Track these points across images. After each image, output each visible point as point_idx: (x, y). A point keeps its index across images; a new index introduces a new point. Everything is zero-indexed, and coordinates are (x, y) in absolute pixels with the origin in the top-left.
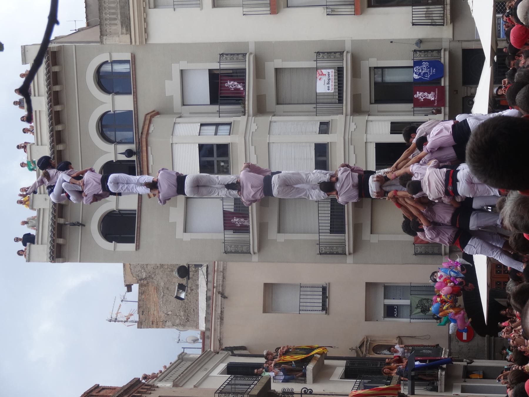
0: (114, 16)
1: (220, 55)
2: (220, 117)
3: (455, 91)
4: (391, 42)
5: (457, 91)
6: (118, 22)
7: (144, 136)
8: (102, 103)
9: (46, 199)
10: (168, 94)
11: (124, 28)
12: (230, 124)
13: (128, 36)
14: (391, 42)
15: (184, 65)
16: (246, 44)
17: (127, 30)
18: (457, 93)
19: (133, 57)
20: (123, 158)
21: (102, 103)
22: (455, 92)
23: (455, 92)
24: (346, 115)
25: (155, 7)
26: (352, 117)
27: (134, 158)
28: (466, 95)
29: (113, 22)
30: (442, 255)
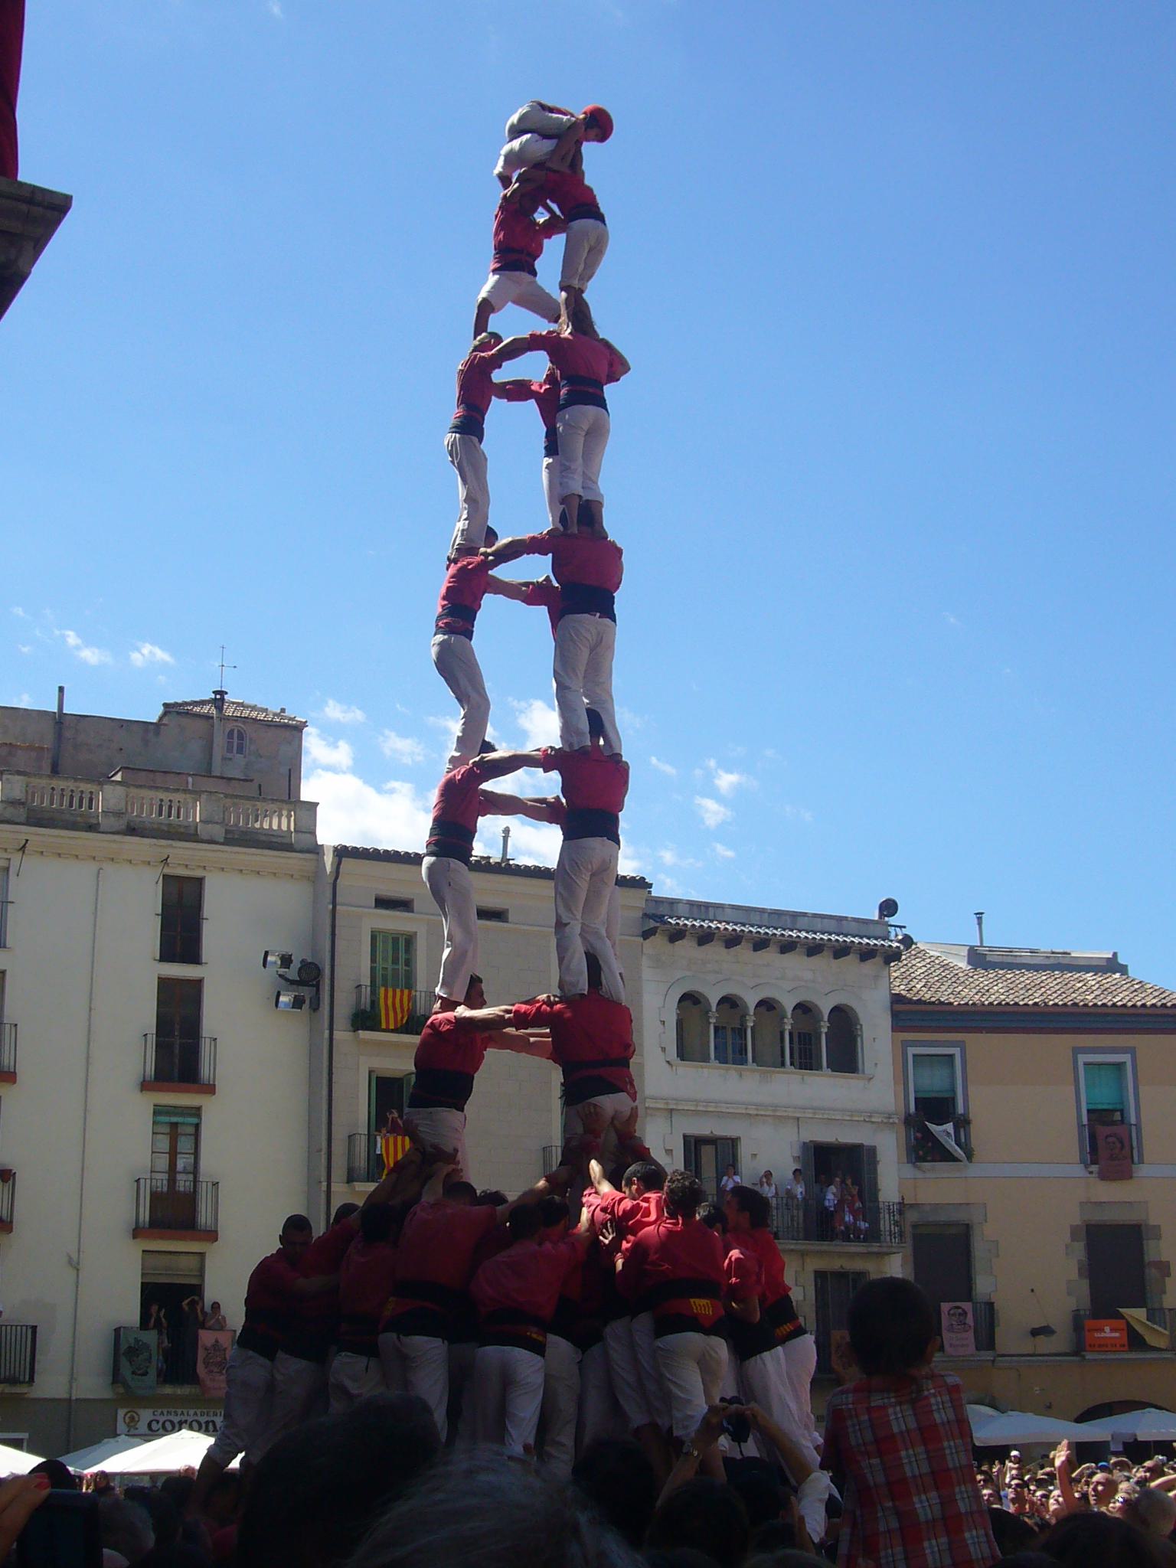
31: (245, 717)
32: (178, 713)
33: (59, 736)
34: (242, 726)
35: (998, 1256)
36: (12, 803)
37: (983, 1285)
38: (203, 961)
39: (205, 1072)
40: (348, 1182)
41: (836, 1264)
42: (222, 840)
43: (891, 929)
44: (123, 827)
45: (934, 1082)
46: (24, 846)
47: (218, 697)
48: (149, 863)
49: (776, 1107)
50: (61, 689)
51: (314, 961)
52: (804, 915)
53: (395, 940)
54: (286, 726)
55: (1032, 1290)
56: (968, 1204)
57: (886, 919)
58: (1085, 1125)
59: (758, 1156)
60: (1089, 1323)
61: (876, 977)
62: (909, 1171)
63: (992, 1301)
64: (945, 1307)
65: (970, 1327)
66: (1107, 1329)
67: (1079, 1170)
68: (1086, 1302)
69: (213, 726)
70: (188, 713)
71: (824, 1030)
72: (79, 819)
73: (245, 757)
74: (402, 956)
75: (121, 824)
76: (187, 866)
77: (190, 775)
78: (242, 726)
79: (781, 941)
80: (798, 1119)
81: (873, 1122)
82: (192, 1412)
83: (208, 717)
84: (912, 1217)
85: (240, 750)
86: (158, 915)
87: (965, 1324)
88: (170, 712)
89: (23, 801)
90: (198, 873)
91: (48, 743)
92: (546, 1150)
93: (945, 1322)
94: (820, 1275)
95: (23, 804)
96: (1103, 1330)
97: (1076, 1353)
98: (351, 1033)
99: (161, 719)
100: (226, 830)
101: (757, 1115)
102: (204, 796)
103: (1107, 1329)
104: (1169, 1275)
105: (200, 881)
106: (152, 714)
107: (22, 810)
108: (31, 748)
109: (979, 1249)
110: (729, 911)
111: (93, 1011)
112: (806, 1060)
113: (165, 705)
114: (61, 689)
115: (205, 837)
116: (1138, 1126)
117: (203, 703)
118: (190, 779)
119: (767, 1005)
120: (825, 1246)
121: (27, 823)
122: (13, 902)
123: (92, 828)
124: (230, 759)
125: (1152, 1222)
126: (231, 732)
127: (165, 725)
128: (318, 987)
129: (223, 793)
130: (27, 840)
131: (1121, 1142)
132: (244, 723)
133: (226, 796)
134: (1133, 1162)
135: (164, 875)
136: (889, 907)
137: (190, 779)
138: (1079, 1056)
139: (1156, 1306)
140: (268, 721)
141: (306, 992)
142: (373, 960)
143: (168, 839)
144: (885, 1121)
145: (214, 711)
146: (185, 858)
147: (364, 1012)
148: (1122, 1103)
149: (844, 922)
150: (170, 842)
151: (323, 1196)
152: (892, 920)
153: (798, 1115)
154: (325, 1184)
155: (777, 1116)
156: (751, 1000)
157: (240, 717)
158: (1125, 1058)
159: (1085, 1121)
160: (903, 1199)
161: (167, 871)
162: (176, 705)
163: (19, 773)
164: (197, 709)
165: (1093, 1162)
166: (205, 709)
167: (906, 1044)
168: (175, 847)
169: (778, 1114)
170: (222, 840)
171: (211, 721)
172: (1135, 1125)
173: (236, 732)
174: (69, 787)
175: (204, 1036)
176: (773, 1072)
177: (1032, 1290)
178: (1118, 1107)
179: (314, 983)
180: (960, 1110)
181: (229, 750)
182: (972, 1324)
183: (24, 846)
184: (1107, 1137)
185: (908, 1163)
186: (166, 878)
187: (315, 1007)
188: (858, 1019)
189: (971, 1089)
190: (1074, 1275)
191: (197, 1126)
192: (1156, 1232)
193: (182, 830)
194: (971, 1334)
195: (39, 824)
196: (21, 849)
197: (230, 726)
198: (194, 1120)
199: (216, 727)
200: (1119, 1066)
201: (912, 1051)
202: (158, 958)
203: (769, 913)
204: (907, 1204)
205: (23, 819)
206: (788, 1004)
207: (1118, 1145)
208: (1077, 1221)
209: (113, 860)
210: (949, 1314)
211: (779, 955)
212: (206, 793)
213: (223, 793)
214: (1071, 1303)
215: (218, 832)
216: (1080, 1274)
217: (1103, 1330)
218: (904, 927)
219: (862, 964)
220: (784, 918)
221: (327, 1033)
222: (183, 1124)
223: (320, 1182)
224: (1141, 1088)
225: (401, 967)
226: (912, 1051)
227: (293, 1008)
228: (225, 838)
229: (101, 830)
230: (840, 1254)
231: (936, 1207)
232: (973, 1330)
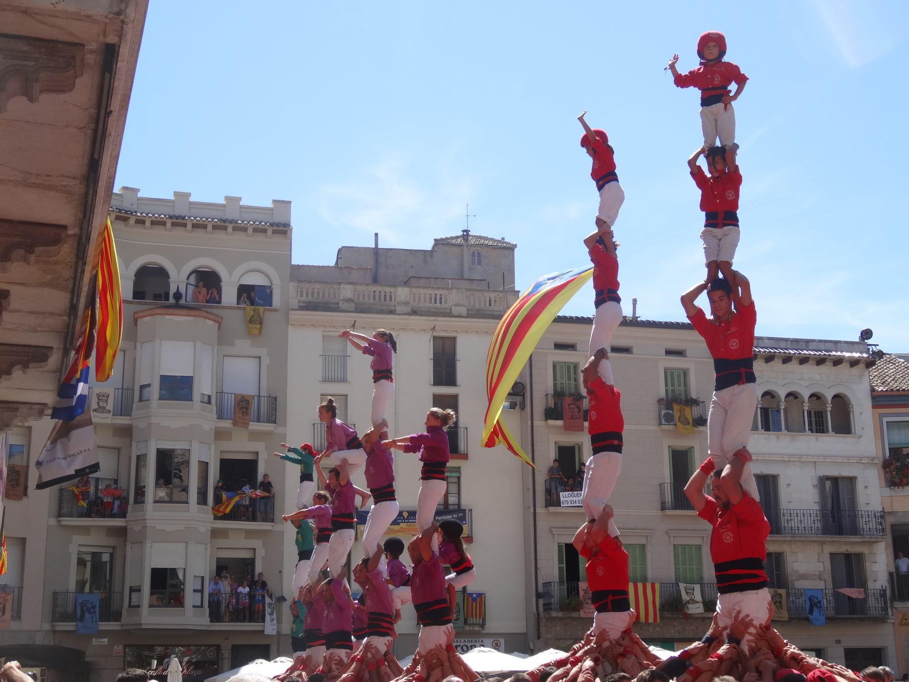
0: (315, 296)
1: (276, 398)
2: (216, 393)
3: (228, 636)
4: (280, 572)
5: (227, 639)
6: (310, 299)
7: (205, 314)
8: (230, 274)
9: (132, 204)
10: (237, 342)
11: (304, 305)
12: (209, 402)
13: (297, 308)
14: (280, 572)
15: (266, 361)
16: (284, 424)
17: (302, 307)
18: (226, 639)
19: (276, 310)
20: (173, 290)
21: (230, 274)
22: (226, 637)
23: (226, 637)
24: (213, 523)
25: (323, 336)
26: (211, 529)
27: (172, 300)
28: (222, 648)
29: (299, 294)
30: (52, 622)
31: (481, 244)
32: (443, 244)
33: (377, 261)
34: (480, 249)
36: (347, 300)
38: (458, 384)
39: (462, 447)
40: (546, 507)
41: (843, 549)
42: (465, 315)
43: (870, 347)
44: (410, 311)
46: (354, 325)
47: (465, 233)
48: (425, 330)
49: (801, 456)
50: (376, 235)
51: (522, 382)
52: (813, 341)
53: (569, 367)
54: (505, 248)
57: (866, 341)
59: (791, 486)
61: (861, 376)
62: (887, 491)
69: (463, 250)
70: (448, 244)
71: (829, 409)
72: (384, 307)
73: (482, 267)
74: (572, 376)
75: (408, 309)
76: (446, 331)
77: (450, 279)
78: (480, 249)
79: (799, 357)
80: (815, 462)
81: (862, 463)
82: (462, 640)
83: (460, 245)
84: (890, 520)
85: (479, 263)
86: (431, 359)
88: (438, 244)
89: (352, 299)
90: (453, 335)
91: (370, 264)
92: (661, 485)
94: (833, 555)
95: (353, 301)
98: (543, 422)
99: (433, 248)
100: (468, 309)
101: (789, 461)
102: (454, 291)
105: (454, 339)
106: (428, 246)
107: (352, 304)
108: (360, 269)
110: (766, 341)
111: (397, 415)
112: (818, 425)
113: (436, 240)
114: (376, 235)
115: (456, 314)
117: (457, 237)
118: (450, 281)
119: (792, 395)
120: (836, 538)
121: (356, 311)
122: (350, 356)
123: (392, 312)
124: (474, 268)
126: (474, 253)
127: (436, 251)
128: (523, 396)
129: (464, 288)
130: (355, 321)
132: (481, 248)
133: (467, 290)
135: (433, 337)
136: (867, 334)
137: (450, 281)
140: (494, 245)
141: (518, 399)
142: (555, 379)
143: (434, 316)
144: (870, 462)
145: (463, 242)
146: (445, 327)
147: (550, 408)
149: (839, 344)
150: (435, 318)
151: (532, 516)
152: (869, 342)
153: (814, 460)
154: (532, 509)
155: (801, 461)
156: (782, 393)
157: (478, 244)
160: (883, 509)
161: (435, 334)
162: (442, 239)
163: (350, 283)
164: (454, 241)
166: (459, 241)
167: (881, 416)
168: (439, 321)
169: (803, 460)
170: (465, 315)
171: (462, 248)
173: (476, 253)
174: (377, 290)
175: (460, 426)
176: (799, 435)
179: (522, 394)
181: (473, 263)
183: (354, 325)
186: (435, 338)
187: (523, 407)
188: (850, 402)
191: (459, 478)
193: (443, 311)
195: (362, 311)
196: (352, 326)
197: (473, 249)
198: (457, 475)
199: (464, 251)
201: (885, 420)
202: (432, 384)
203: (791, 341)
204: (886, 512)
205: (353, 309)
206: (806, 394)
209: (404, 329)
211: (799, 366)
212: (455, 289)
213: (464, 288)
215: (463, 311)
218: (878, 345)
219: (851, 369)
220: (800, 343)
221: (530, 422)
222: (450, 477)
223: (530, 508)
225: (572, 382)
226: (885, 420)
227: (510, 408)
228: (467, 314)
229: (397, 313)
230: (846, 543)
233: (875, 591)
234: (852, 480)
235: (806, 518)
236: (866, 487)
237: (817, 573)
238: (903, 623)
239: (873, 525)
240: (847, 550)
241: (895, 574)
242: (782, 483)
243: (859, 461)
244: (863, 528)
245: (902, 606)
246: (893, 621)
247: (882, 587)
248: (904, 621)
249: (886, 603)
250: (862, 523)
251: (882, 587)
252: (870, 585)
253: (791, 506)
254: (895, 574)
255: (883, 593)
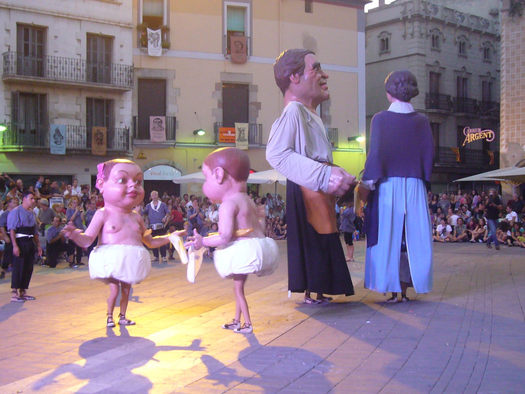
35: (179, 96)
37: (171, 109)
45: (153, 10)
55: (195, 113)
56: (166, 70)
58: (225, 36)
60: (221, 129)
62: (138, 52)
63: (176, 116)
64: (152, 118)
65: (164, 129)
66: (230, 132)
67: (220, 57)
68: (220, 120)
84: (138, 74)
87: (161, 127)
93: (151, 127)
96: (227, 132)
97: (214, 143)
103: (230, 132)
104: (260, 109)
109: (170, 92)
116: (251, 38)
125: (255, 83)
131: (242, 45)
134: (247, 55)
138: (225, 2)
139: (253, 123)
148: (244, 28)
158: (247, 5)
159: (226, 33)
160: (133, 64)
165: (229, 53)
172: (249, 37)
177: (195, 113)
178: (242, 30)
180: (165, 23)
182: (165, 127)
184: (235, 42)
185: (138, 48)
189: (171, 14)
190: (216, 106)
192: (256, 88)
194: (164, 132)
200: (244, 9)
204: (135, 68)
207: (240, 46)
208: (219, 81)
210: (154, 122)
214: (214, 120)
216: (219, 106)
217: (227, 132)
224: (254, 20)
231: (150, 70)
232: (165, 130)
233: (120, 131)
234: (109, 40)
235: (67, 66)
236: (122, 46)
237: (74, 113)
238: (140, 156)
239: (124, 78)
240: (101, 96)
241: (137, 118)
242: (50, 34)
243: (118, 24)
244: (115, 79)
245: (140, 143)
246: (132, 155)
247: (126, 127)
248: (141, 155)
249: (128, 140)
250: (115, 74)
251: (126, 127)
252: (117, 126)
253: (56, 55)
254: (137, 118)
255: (126, 132)
